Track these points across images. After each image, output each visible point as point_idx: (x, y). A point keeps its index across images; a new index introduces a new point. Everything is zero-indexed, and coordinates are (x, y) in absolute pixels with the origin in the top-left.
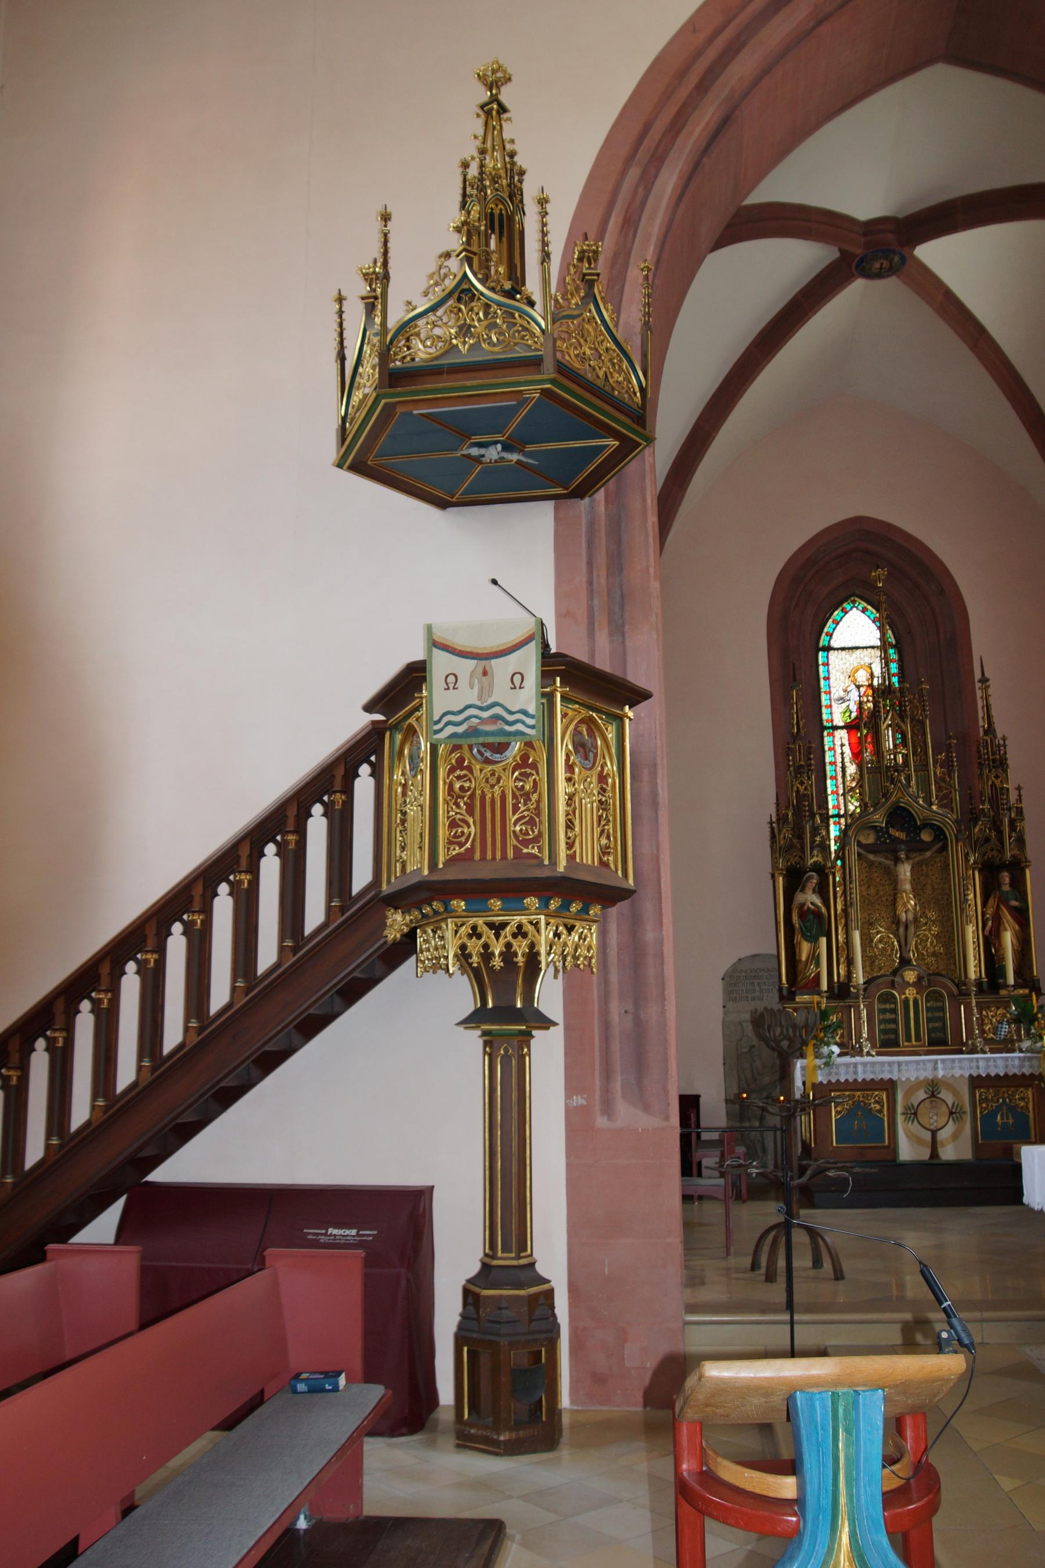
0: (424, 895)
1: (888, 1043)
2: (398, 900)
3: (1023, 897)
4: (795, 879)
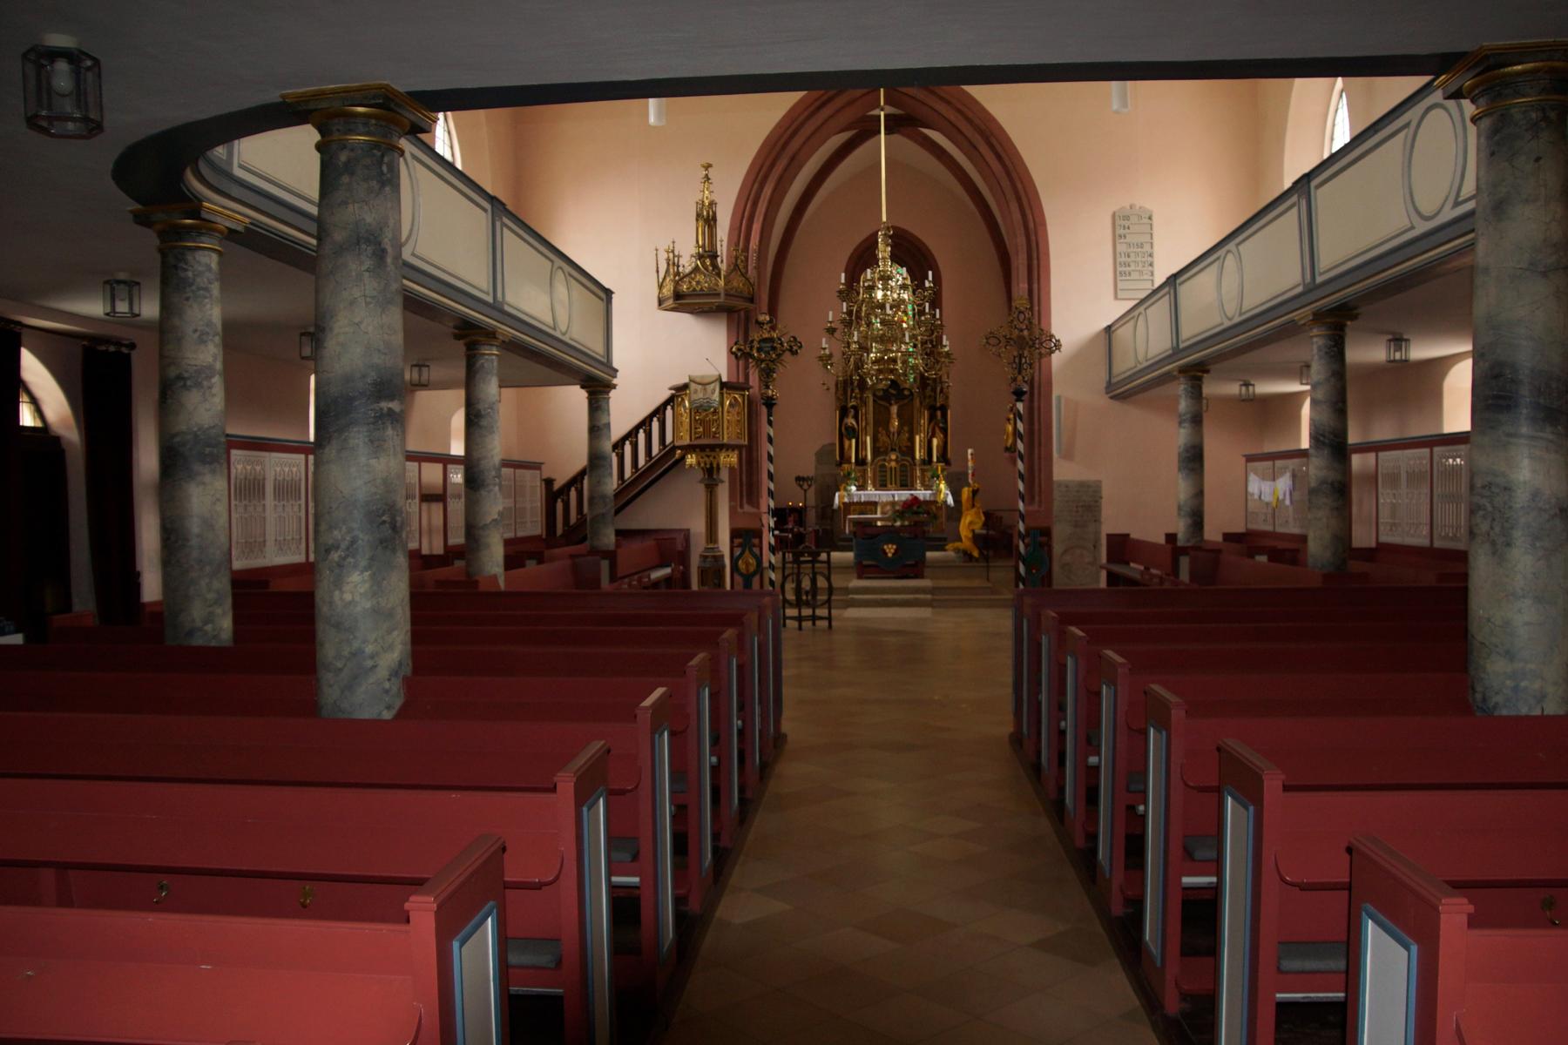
0: (690, 449)
1: (882, 485)
2: (679, 448)
3: (946, 422)
4: (844, 412)
